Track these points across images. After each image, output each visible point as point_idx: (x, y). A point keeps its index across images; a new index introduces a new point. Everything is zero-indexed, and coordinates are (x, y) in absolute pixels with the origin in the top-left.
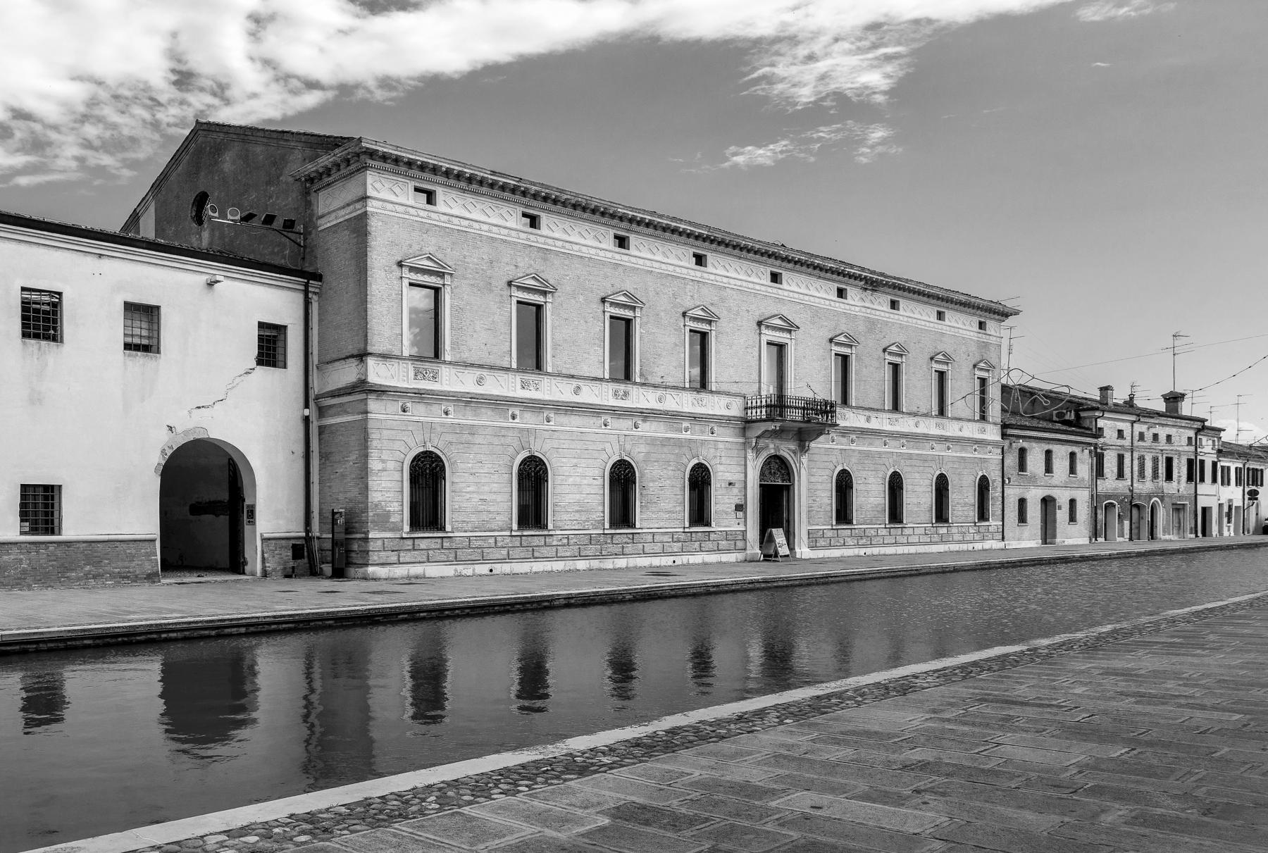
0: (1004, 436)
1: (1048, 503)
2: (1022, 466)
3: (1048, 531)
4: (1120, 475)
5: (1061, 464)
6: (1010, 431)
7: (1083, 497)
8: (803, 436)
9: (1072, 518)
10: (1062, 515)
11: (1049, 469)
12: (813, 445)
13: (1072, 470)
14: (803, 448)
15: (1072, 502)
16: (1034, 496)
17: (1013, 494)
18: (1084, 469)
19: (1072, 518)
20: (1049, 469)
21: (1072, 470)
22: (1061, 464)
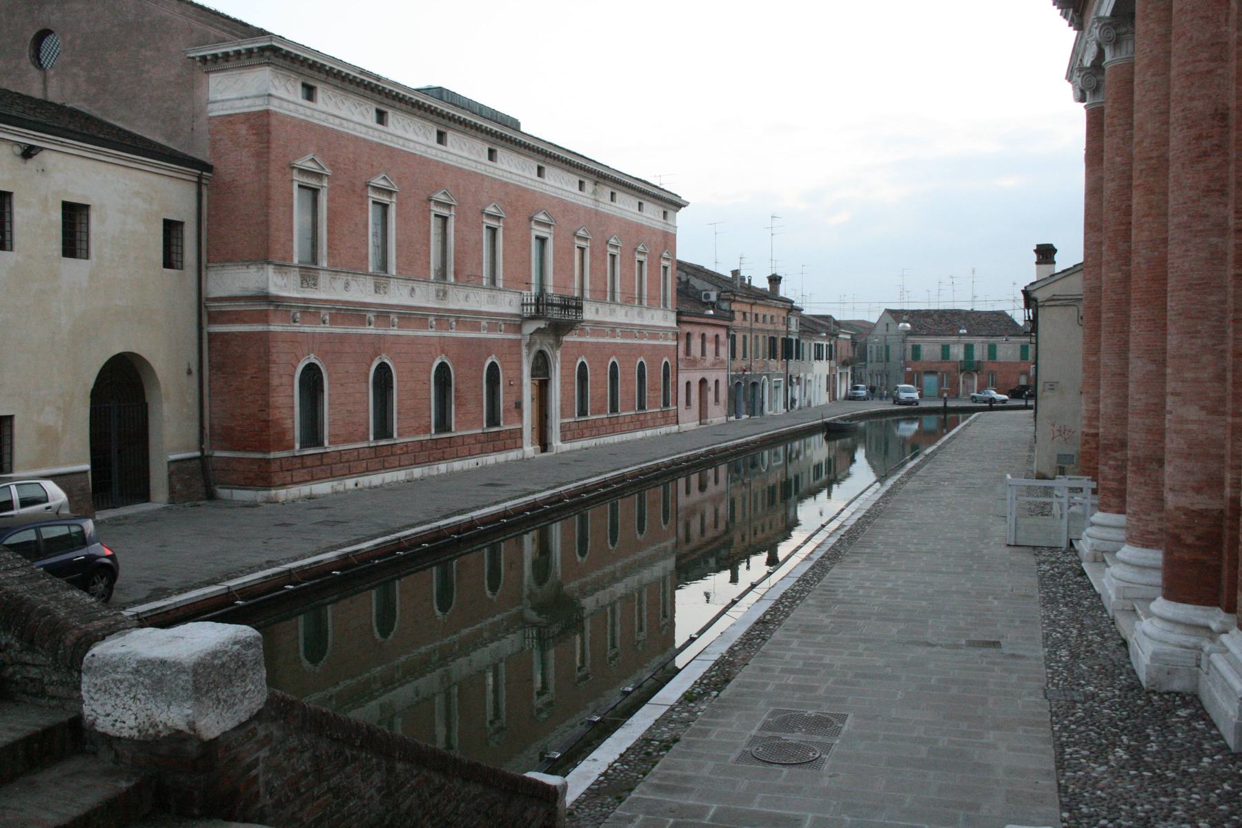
0: (679, 322)
1: (703, 382)
2: (688, 352)
3: (703, 414)
4: (745, 356)
5: (710, 347)
6: (685, 318)
7: (722, 376)
8: (558, 329)
9: (717, 400)
10: (711, 396)
11: (703, 353)
12: (566, 339)
13: (717, 353)
14: (558, 343)
15: (717, 381)
16: (695, 377)
17: (683, 378)
18: (724, 352)
19: (717, 400)
20: (703, 353)
21: (717, 353)
22: (710, 347)
